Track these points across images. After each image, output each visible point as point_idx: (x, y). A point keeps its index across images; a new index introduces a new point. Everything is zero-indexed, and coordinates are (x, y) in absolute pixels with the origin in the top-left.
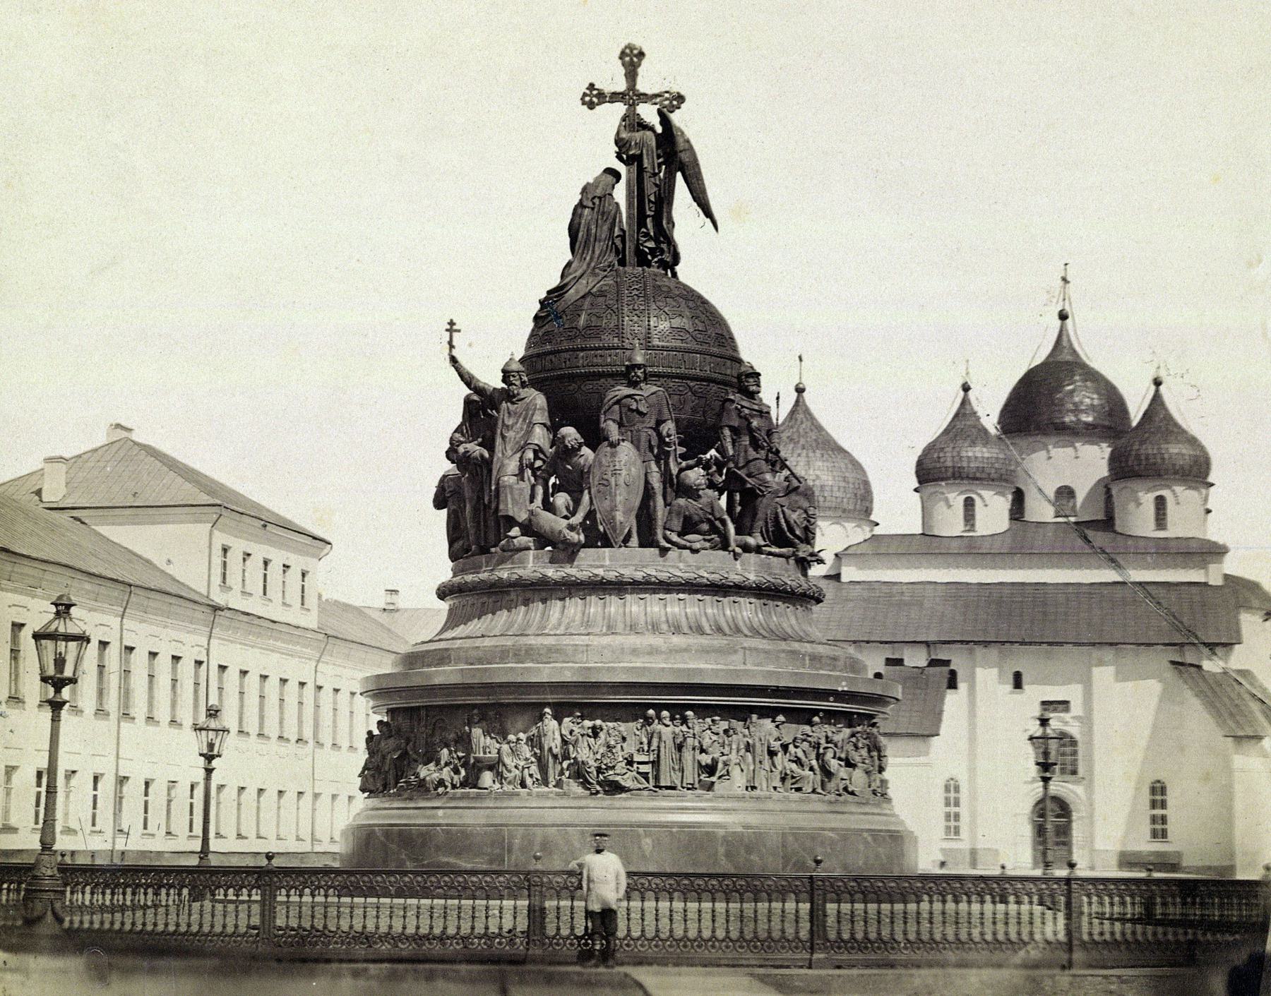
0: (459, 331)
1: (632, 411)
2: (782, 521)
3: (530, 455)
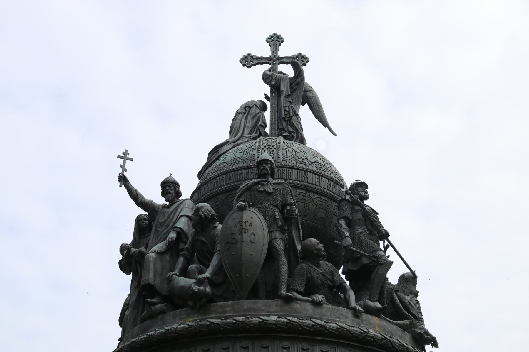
0: (131, 159)
1: (262, 192)
2: (398, 302)
3: (173, 235)
